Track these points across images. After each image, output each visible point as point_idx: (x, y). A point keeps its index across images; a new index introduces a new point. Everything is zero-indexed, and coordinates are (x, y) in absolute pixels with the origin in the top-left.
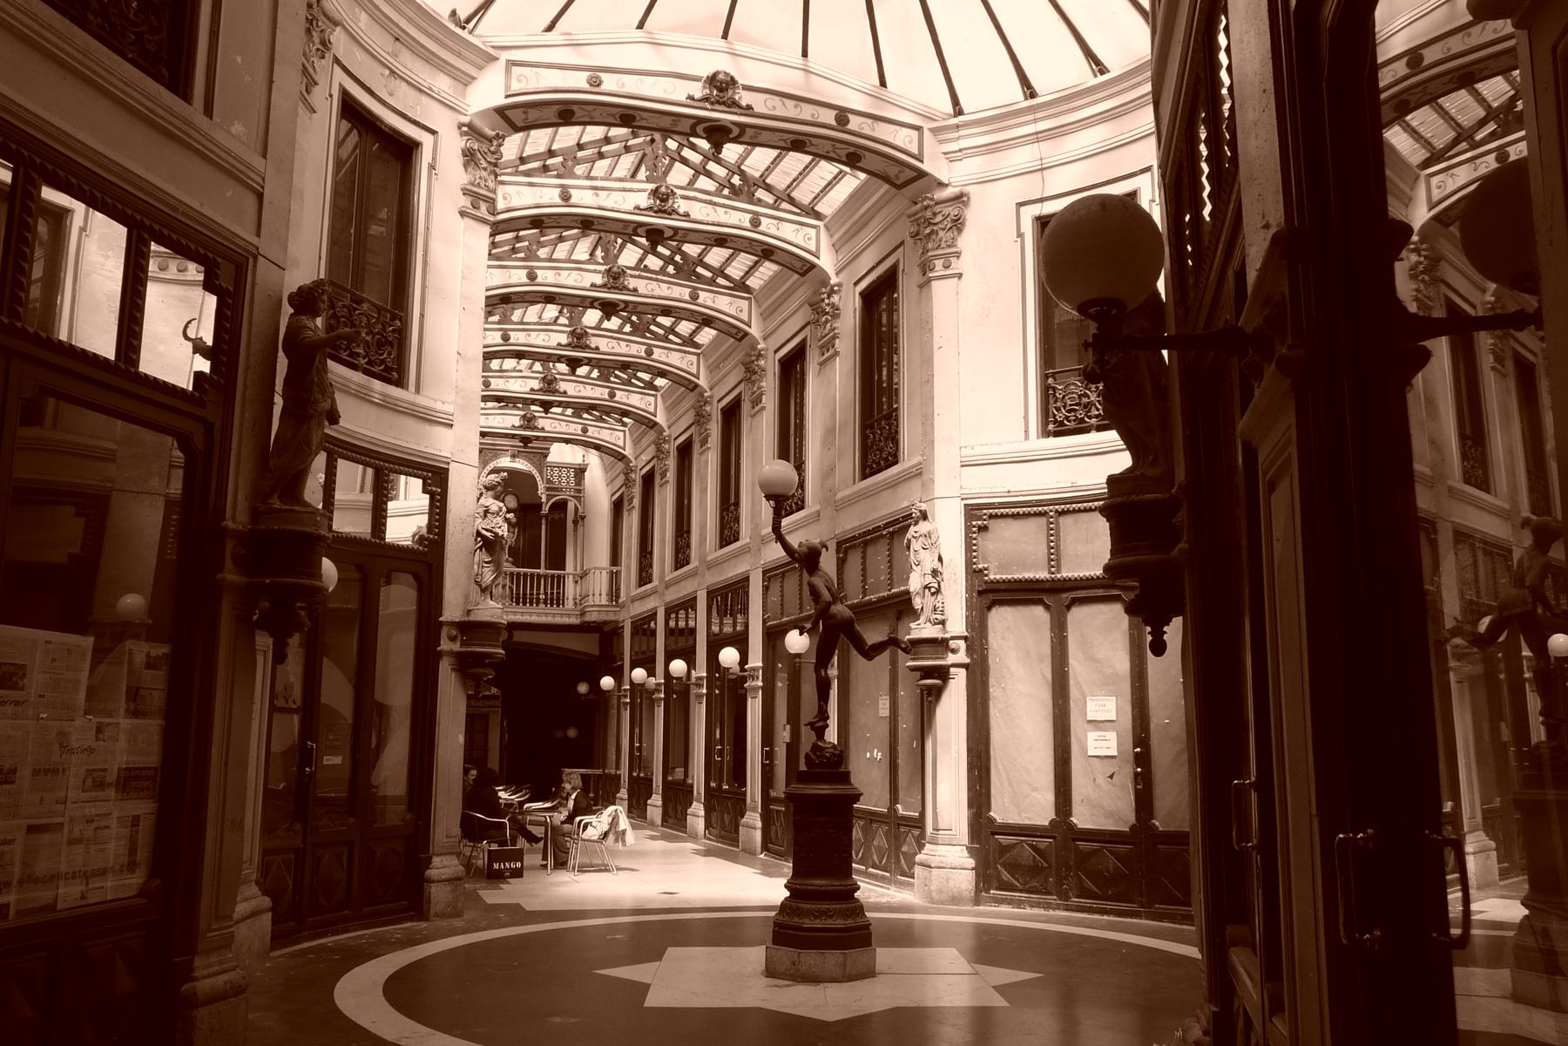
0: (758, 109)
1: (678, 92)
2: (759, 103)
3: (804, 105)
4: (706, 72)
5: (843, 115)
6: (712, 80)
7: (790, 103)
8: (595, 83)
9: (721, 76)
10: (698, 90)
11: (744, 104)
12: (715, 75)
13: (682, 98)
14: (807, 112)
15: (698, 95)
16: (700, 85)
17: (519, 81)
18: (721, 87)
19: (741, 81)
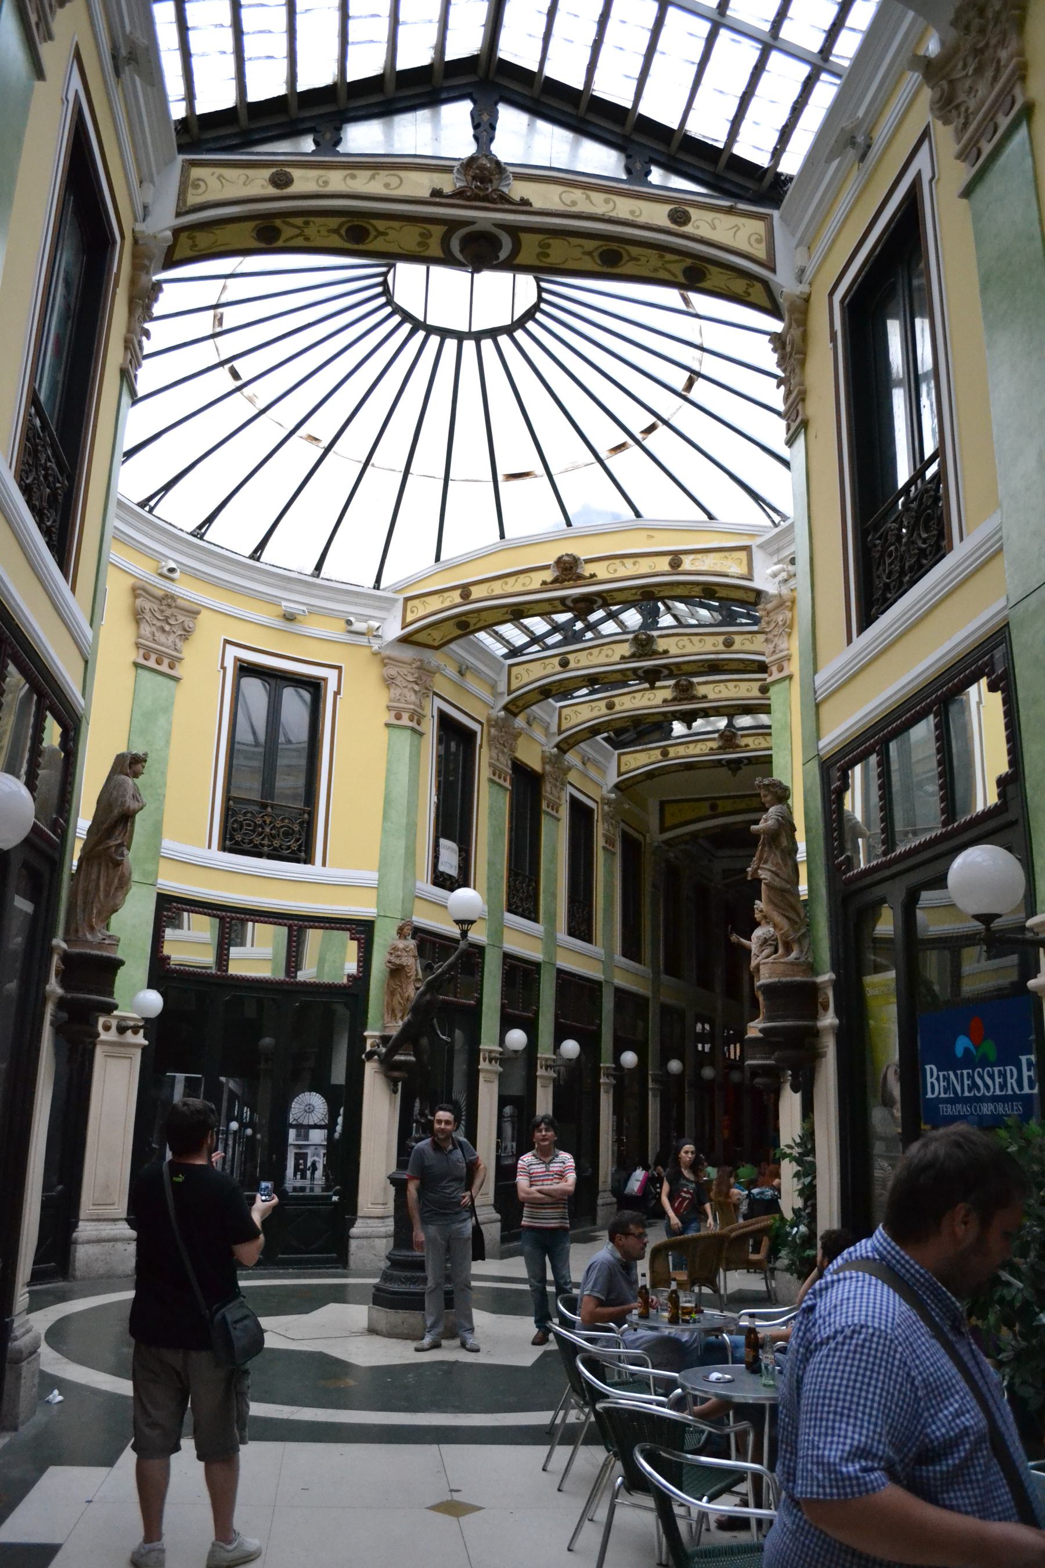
1: (536, 581)
2: (601, 570)
3: (640, 560)
4: (551, 561)
5: (676, 558)
6: (559, 561)
7: (628, 562)
9: (566, 558)
10: (548, 576)
11: (587, 574)
12: (560, 558)
13: (536, 585)
14: (644, 566)
15: (549, 579)
17: (412, 612)
18: (568, 569)
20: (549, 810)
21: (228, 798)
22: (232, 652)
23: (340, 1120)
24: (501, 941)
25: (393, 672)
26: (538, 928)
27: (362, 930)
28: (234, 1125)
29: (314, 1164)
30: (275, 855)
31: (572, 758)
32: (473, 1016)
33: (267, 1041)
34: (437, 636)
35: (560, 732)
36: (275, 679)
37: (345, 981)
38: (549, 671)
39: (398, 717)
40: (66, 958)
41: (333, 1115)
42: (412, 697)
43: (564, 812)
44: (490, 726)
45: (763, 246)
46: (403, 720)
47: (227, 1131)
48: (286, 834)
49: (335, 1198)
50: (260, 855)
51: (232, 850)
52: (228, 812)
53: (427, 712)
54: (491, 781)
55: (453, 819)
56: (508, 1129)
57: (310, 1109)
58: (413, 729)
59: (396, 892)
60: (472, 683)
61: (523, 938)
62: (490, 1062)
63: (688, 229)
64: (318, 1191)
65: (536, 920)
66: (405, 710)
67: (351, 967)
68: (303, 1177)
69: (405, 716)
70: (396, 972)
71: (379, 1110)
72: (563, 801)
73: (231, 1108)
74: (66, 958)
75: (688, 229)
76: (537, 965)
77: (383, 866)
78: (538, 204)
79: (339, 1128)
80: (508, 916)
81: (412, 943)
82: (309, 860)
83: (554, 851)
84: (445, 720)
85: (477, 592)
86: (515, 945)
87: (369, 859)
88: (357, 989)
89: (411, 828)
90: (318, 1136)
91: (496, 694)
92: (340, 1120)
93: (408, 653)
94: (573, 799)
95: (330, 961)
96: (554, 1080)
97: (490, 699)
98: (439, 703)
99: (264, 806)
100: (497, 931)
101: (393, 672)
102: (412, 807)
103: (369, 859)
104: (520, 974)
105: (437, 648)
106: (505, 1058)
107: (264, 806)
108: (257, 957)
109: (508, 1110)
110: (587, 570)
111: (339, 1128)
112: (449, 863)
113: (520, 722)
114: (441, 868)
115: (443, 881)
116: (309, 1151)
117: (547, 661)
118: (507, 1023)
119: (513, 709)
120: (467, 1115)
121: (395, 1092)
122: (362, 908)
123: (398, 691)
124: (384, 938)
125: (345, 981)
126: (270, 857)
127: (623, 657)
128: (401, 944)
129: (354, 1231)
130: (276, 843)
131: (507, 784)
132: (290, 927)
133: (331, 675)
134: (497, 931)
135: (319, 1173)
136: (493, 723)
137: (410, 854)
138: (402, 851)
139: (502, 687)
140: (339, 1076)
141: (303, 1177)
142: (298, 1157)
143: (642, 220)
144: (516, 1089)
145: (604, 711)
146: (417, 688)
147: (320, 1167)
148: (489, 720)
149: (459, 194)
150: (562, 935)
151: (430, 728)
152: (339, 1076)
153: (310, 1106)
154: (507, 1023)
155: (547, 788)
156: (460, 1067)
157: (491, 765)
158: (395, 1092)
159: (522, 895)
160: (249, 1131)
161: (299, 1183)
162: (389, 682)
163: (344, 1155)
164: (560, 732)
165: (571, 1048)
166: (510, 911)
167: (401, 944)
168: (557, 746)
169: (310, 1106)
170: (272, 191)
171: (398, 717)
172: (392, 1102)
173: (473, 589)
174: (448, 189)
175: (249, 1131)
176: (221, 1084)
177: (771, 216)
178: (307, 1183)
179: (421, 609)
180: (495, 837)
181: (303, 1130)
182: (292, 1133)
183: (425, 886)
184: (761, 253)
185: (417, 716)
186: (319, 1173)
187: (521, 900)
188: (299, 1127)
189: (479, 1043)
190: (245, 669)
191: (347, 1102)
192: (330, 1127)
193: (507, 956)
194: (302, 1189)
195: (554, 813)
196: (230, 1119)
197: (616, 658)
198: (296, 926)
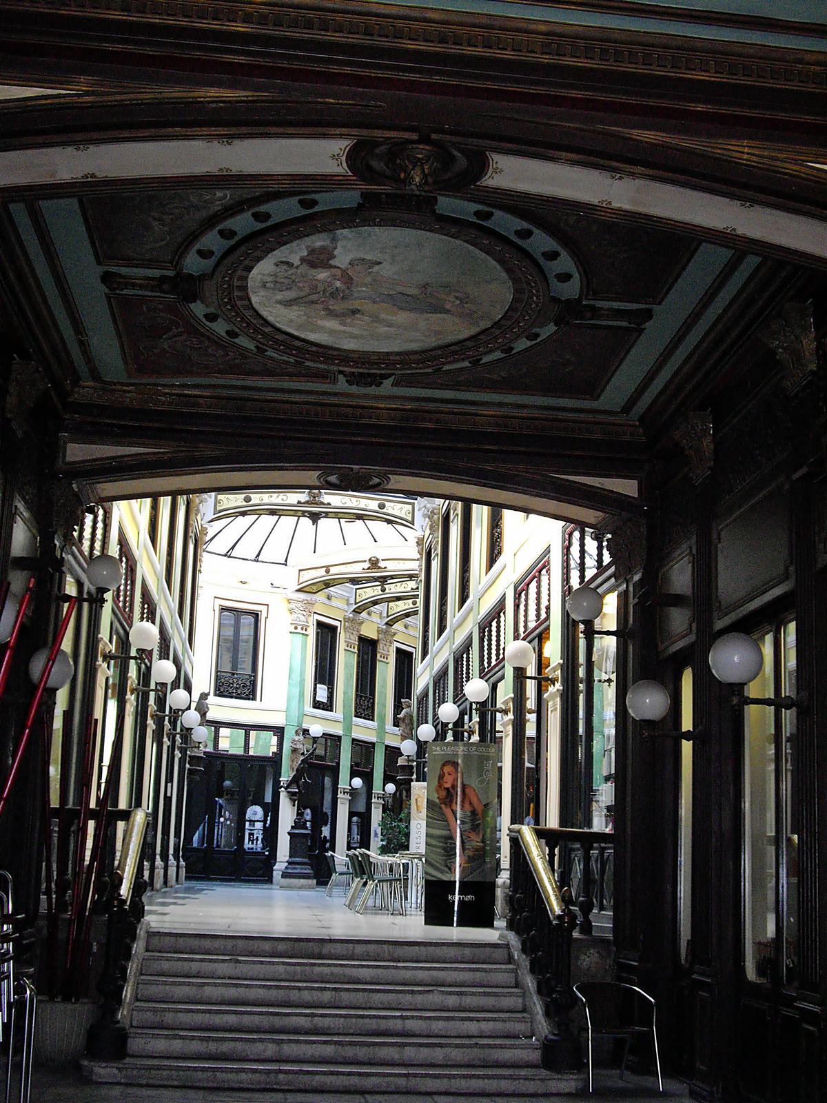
0: (388, 569)
1: (358, 568)
2: (391, 566)
8: (328, 571)
10: (367, 565)
16: (367, 563)
19: (380, 558)
20: (382, 659)
21: (217, 672)
22: (219, 602)
23: (269, 818)
24: (351, 732)
25: (293, 606)
26: (374, 724)
27: (279, 731)
28: (222, 820)
29: (257, 837)
30: (239, 697)
31: (398, 626)
32: (335, 772)
33: (227, 783)
34: (315, 588)
35: (388, 616)
36: (238, 612)
37: (271, 755)
38: (376, 593)
39: (296, 628)
40: (190, 756)
41: (266, 816)
42: (303, 618)
43: (392, 659)
44: (345, 621)
45: (410, 515)
46: (298, 630)
47: (219, 822)
48: (244, 687)
49: (267, 853)
50: (232, 697)
51: (219, 696)
52: (217, 678)
53: (310, 624)
54: (345, 650)
55: (325, 673)
56: (355, 829)
57: (255, 813)
58: (303, 634)
59: (295, 713)
60: (335, 602)
61: (364, 730)
62: (344, 793)
63: (384, 510)
64: (259, 850)
65: (373, 720)
66: (299, 624)
67: (274, 749)
68: (253, 843)
69: (299, 627)
70: (294, 751)
71: (287, 814)
72: (391, 652)
73: (220, 812)
74: (190, 756)
75: (384, 510)
76: (373, 744)
77: (289, 700)
78: (333, 504)
79: (268, 822)
80: (355, 719)
81: (301, 737)
82: (254, 699)
83: (385, 681)
84: (320, 625)
85: (333, 570)
86: (358, 734)
87: (284, 696)
88: (276, 760)
89: (302, 681)
90: (259, 825)
91: (348, 604)
92: (269, 818)
93: (302, 596)
94: (398, 650)
95: (264, 745)
96: (383, 805)
97: (346, 607)
98: (317, 617)
99: (233, 674)
100: (349, 727)
101: (293, 606)
102: (302, 672)
103: (284, 696)
104: (364, 750)
105: (314, 593)
106: (353, 792)
107: (233, 674)
108: (229, 742)
109: (355, 819)
110: (382, 564)
111: (268, 822)
112: (322, 694)
113: (364, 614)
114: (317, 699)
115: (317, 705)
116: (255, 832)
117: (375, 588)
118: (353, 774)
119: (357, 611)
120: (332, 819)
121: (294, 806)
122: (278, 720)
123: (296, 615)
124: (289, 735)
125: (271, 755)
126: (236, 698)
127: (412, 589)
128: (297, 738)
129: (275, 868)
130: (239, 692)
131: (356, 650)
132: (246, 730)
133: (264, 609)
134: (349, 727)
135: (259, 842)
136: (347, 619)
137: (302, 695)
138: (298, 693)
139: (352, 601)
140: (268, 798)
141: (253, 843)
142: (250, 834)
143: (369, 508)
144: (361, 808)
145: (412, 606)
146: (305, 613)
147: (260, 839)
148: (344, 619)
149: (307, 502)
150: (389, 727)
151: (312, 631)
152: (268, 798)
153: (255, 812)
154: (353, 774)
155: (380, 647)
156: (328, 797)
157: (345, 641)
158: (294, 806)
159: (365, 706)
160: (228, 822)
161: (251, 846)
162: (291, 611)
163: (271, 834)
164: (388, 616)
165: (391, 788)
166: (356, 716)
167: (297, 738)
168: (387, 624)
169: (255, 812)
170: (245, 503)
171: (296, 628)
172: (293, 810)
173: (331, 568)
174: (303, 501)
175: (228, 822)
176: (216, 801)
177: (414, 503)
178: (254, 846)
179: (307, 576)
180: (348, 679)
181: (252, 822)
182: (247, 823)
183: (309, 709)
184: (410, 519)
185: (305, 628)
186: (259, 842)
187: (364, 710)
188: (250, 821)
189: (338, 784)
190: (224, 609)
191: (272, 810)
192: (265, 821)
193: (354, 740)
194: (252, 849)
195: (385, 660)
196: (220, 816)
197: (409, 589)
198: (247, 728)
